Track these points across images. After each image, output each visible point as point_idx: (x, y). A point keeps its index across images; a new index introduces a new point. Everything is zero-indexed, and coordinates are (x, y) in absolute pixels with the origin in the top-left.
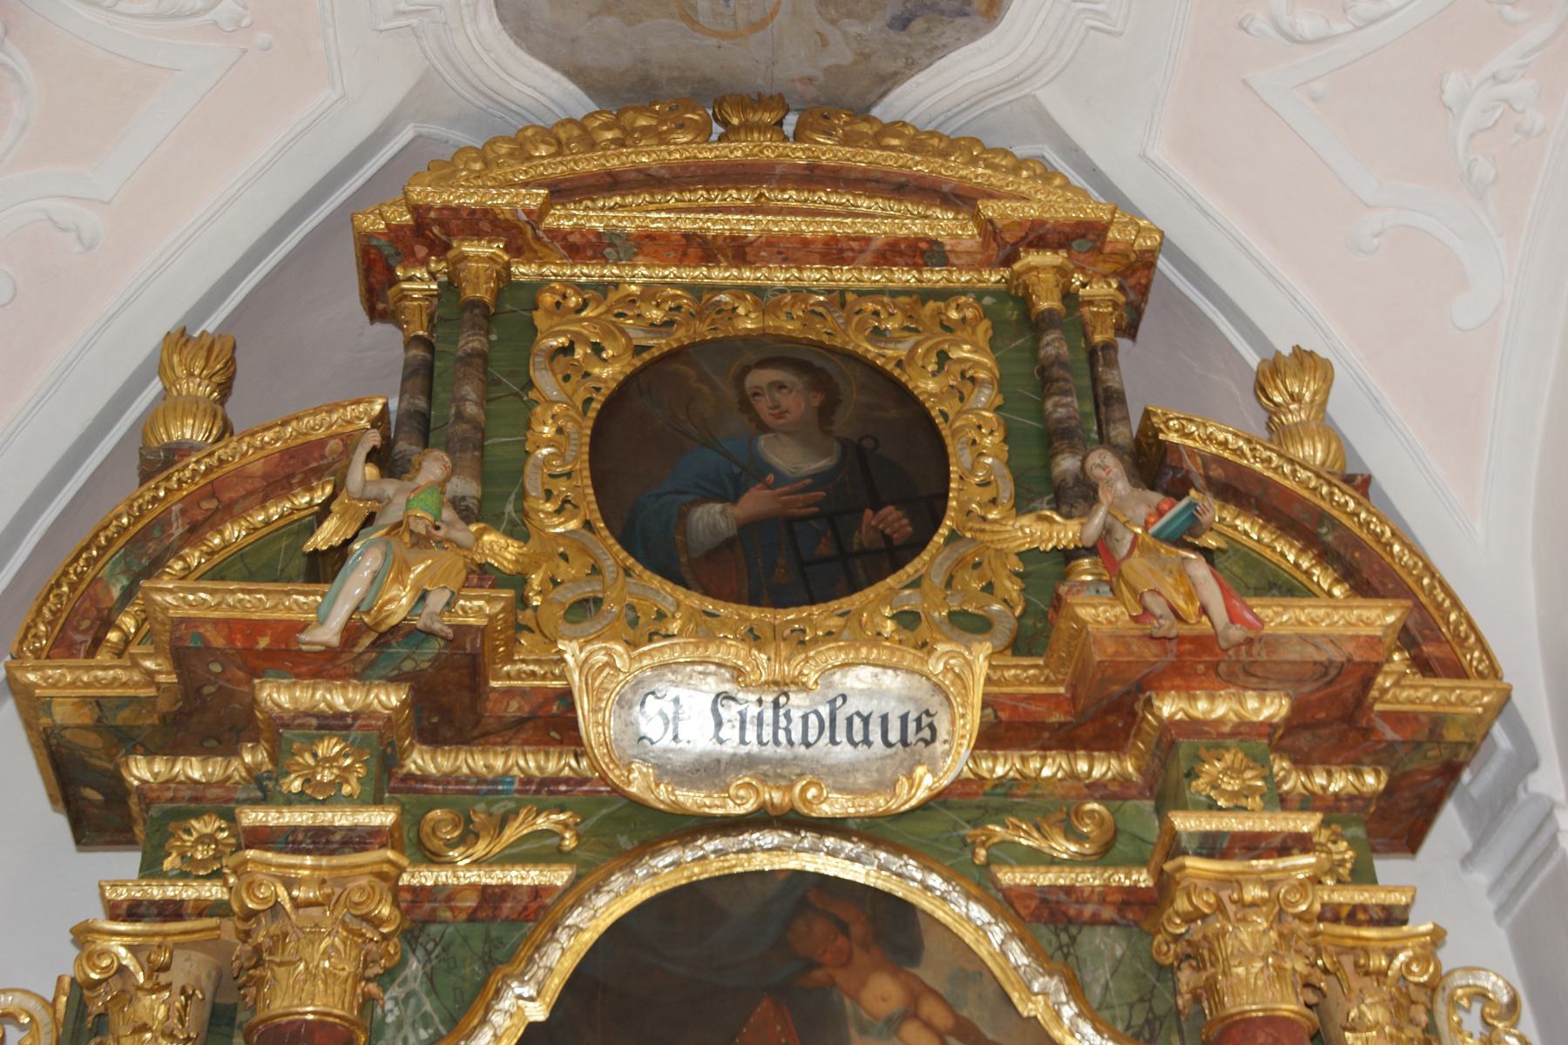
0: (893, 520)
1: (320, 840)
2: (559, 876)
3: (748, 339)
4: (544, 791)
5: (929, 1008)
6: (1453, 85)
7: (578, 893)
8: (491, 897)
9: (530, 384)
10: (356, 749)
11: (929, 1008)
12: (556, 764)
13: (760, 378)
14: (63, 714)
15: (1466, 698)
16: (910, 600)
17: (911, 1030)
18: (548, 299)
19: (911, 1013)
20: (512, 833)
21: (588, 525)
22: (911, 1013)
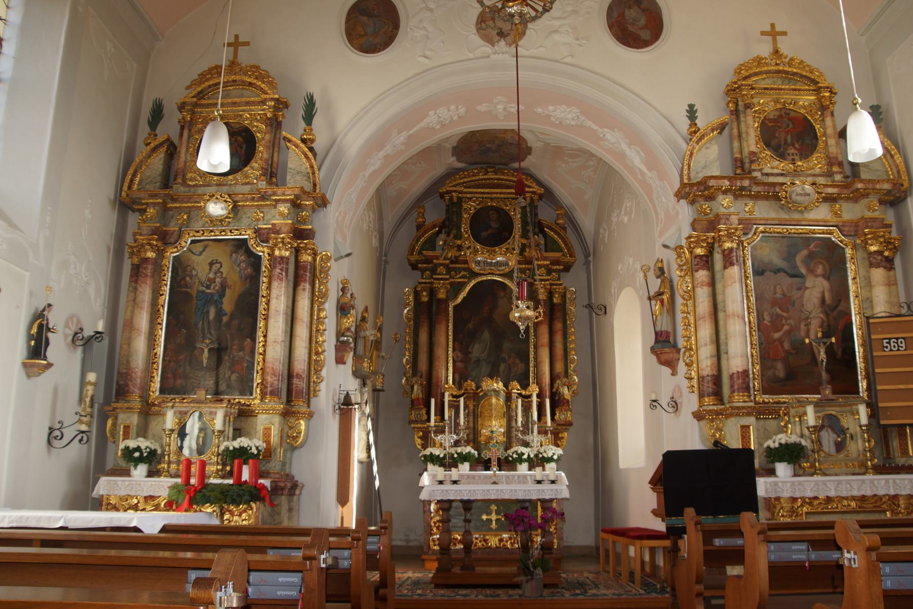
0: (506, 234)
1: (442, 279)
2: (466, 280)
3: (489, 206)
4: (465, 269)
5: (507, 296)
6: (583, 172)
7: (469, 281)
8: (459, 282)
9: (461, 214)
10: (444, 267)
11: (507, 296)
12: (466, 266)
13: (491, 212)
14: (413, 262)
15: (572, 260)
16: (508, 246)
17: (505, 298)
18: (464, 200)
19: (505, 296)
20: (461, 274)
21: (469, 236)
22: (505, 296)
